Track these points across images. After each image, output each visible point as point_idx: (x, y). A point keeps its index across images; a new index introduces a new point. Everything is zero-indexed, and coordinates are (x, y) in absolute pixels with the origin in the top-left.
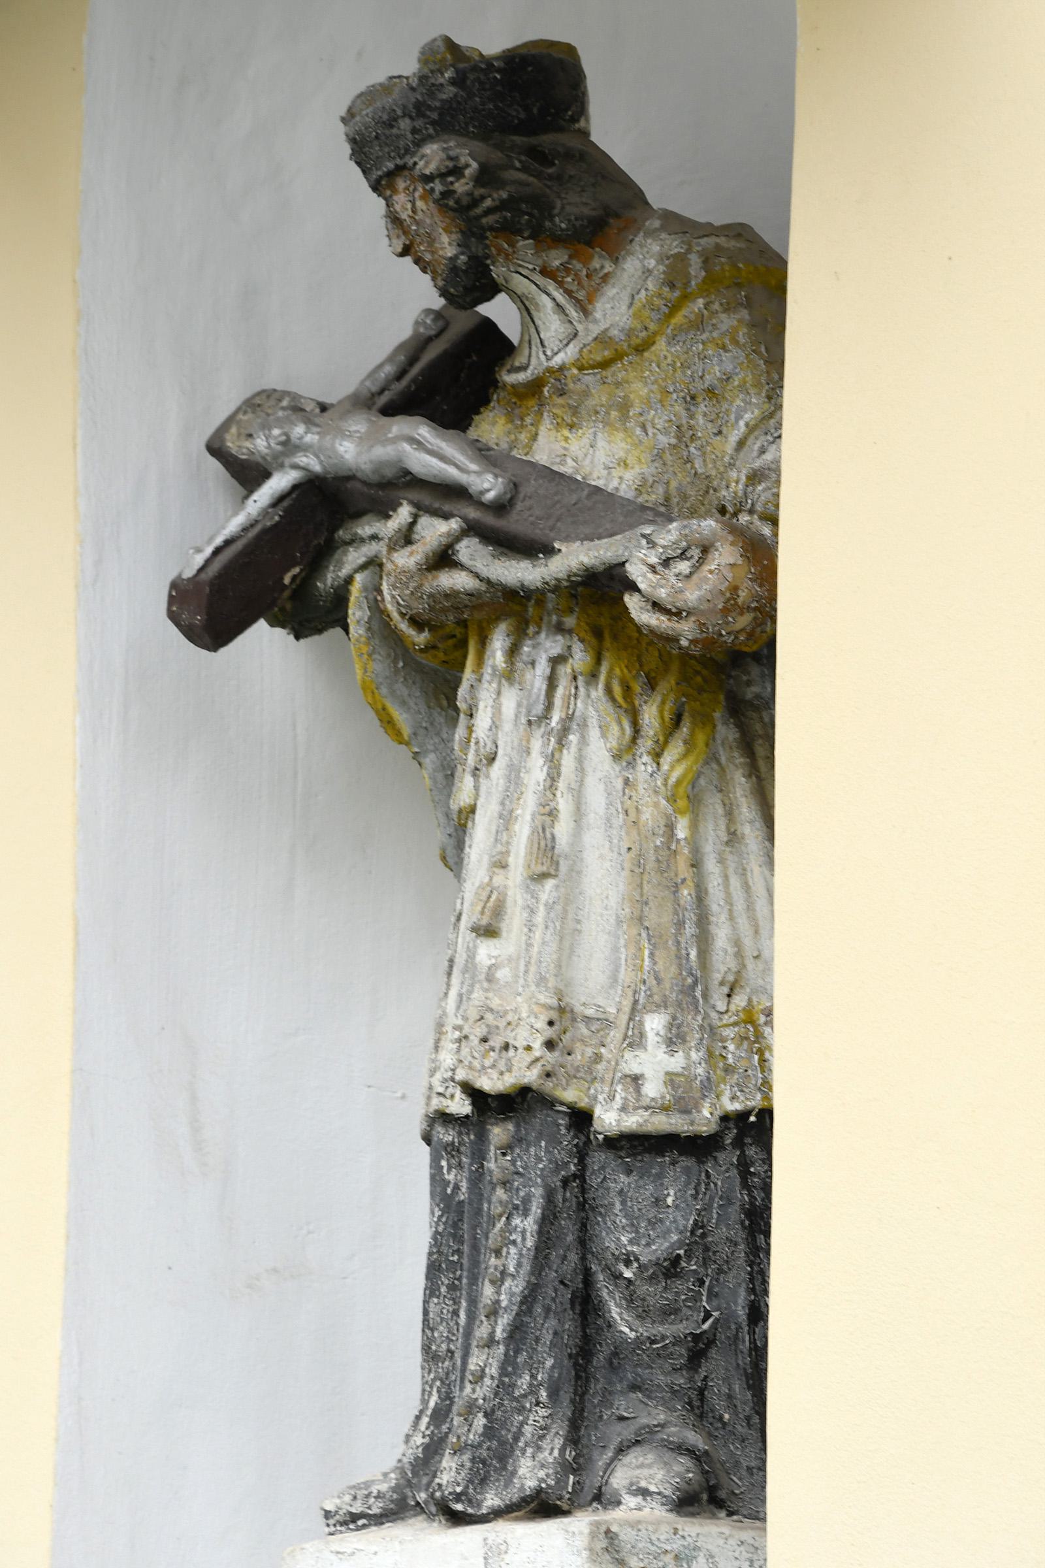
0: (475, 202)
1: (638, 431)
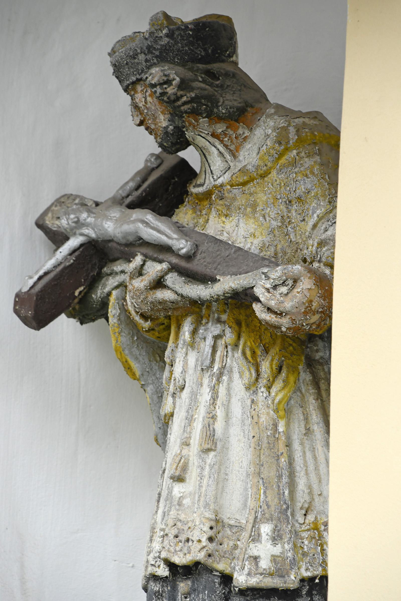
0: (178, 98)
1: (261, 219)
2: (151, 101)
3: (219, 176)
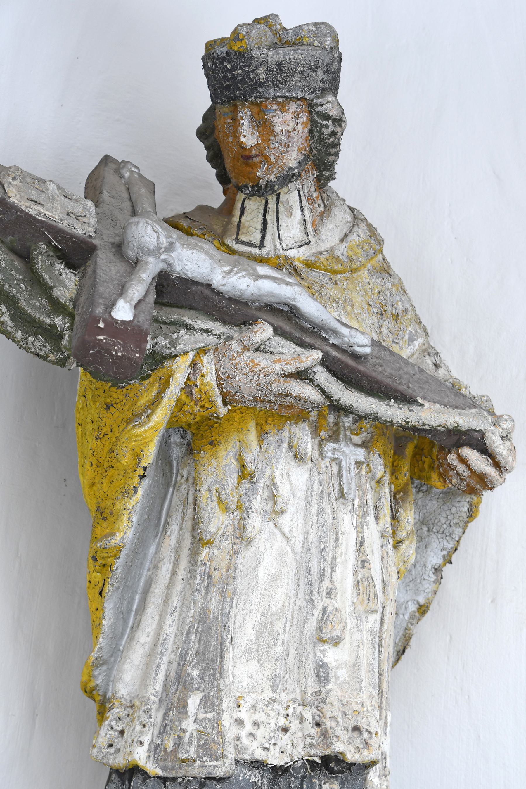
2: (300, 131)
3: (290, 246)
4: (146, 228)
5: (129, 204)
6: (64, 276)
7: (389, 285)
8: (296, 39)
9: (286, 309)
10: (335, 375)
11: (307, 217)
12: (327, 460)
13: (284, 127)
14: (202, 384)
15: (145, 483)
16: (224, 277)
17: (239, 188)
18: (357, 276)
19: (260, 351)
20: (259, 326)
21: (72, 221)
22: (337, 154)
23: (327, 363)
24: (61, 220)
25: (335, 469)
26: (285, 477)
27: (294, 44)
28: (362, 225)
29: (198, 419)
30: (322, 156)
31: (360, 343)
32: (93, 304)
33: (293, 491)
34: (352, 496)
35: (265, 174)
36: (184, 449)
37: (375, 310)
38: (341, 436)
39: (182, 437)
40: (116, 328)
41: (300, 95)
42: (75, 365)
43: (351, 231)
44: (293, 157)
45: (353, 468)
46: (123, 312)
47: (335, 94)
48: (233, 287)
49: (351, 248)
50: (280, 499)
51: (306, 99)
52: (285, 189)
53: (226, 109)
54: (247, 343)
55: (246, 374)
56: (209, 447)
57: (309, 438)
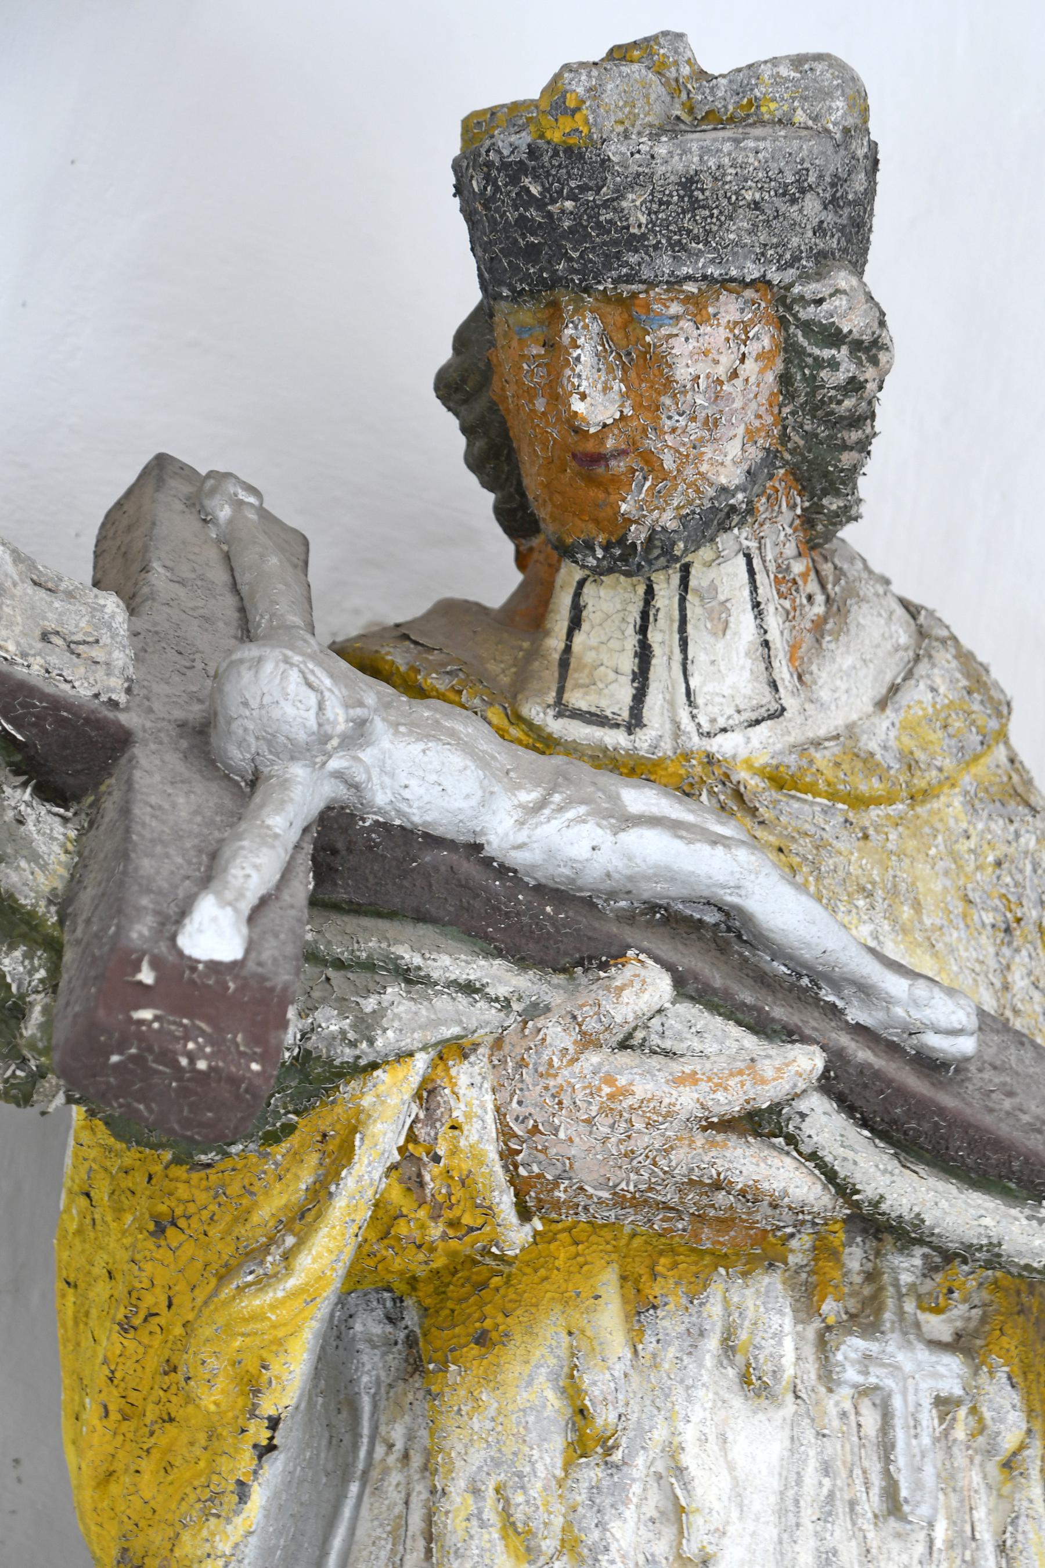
2: (752, 380)
3: (722, 723)
4: (284, 676)
5: (230, 601)
6: (31, 826)
7: (1029, 841)
8: (738, 105)
9: (711, 917)
10: (865, 1124)
11: (774, 636)
12: (846, 1392)
13: (703, 368)
14: (454, 1152)
15: (275, 1467)
16: (521, 823)
17: (566, 551)
18: (931, 812)
19: (631, 1047)
20: (629, 971)
21: (57, 658)
22: (863, 447)
23: (840, 1086)
24: (24, 655)
25: (871, 1420)
26: (713, 1446)
27: (731, 119)
28: (945, 657)
29: (440, 1262)
30: (818, 455)
31: (944, 1023)
32: (120, 911)
33: (738, 1494)
34: (924, 1510)
35: (647, 509)
36: (395, 1359)
37: (989, 918)
38: (888, 1315)
39: (390, 1320)
40: (195, 988)
41: (753, 271)
42: (60, 1099)
43: (909, 675)
44: (730, 458)
45: (928, 1418)
46: (213, 935)
47: (858, 267)
48: (550, 854)
49: (909, 727)
50: (698, 1520)
51: (769, 283)
52: (706, 553)
53: (526, 314)
54: (591, 1025)
55: (589, 1121)
56: (475, 1350)
57: (788, 1322)
